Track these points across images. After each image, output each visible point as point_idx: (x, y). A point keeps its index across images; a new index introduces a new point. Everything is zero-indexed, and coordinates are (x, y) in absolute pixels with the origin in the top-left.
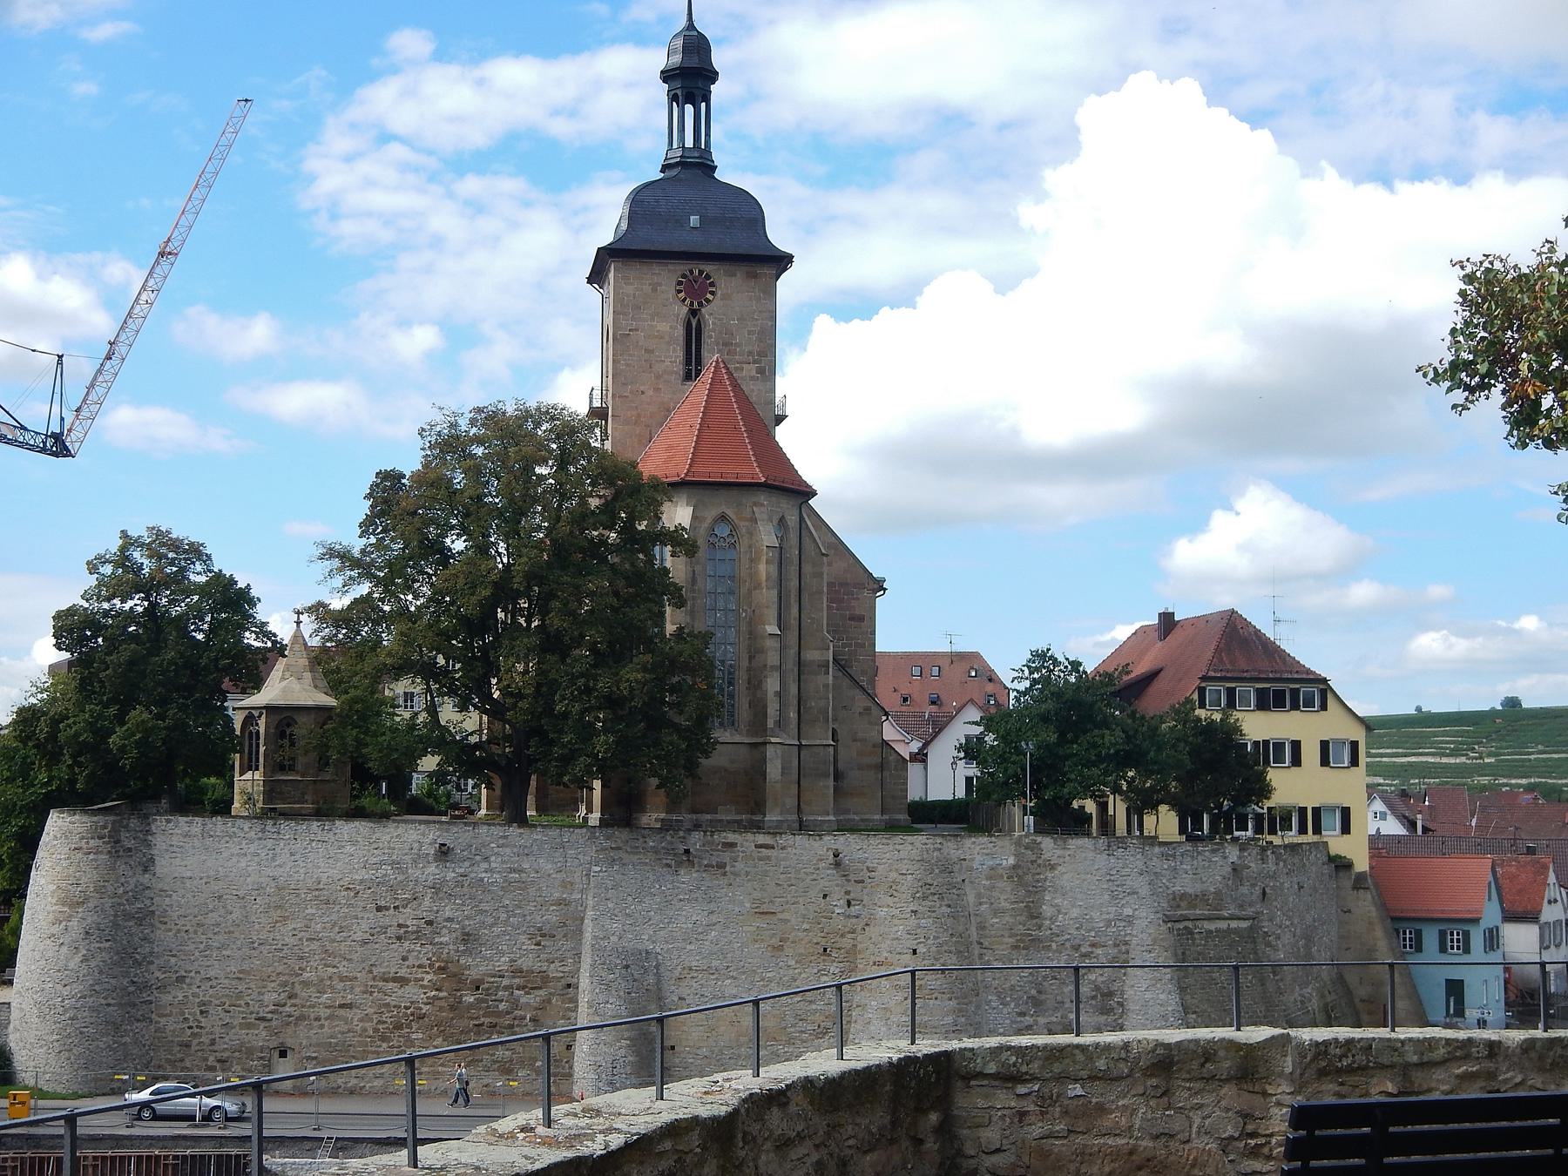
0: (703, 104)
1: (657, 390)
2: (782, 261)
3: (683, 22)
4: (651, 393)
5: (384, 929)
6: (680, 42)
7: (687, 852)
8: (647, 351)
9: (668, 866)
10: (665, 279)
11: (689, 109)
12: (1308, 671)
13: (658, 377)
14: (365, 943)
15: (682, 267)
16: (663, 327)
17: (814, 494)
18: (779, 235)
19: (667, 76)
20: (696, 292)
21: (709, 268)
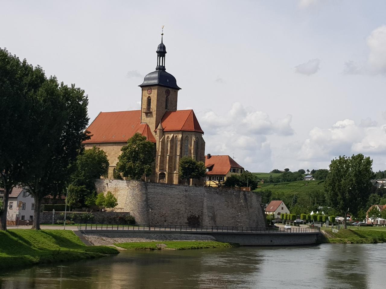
0: (164, 57)
1: (162, 110)
2: (179, 89)
3: (161, 43)
4: (161, 110)
5: (178, 202)
6: (159, 46)
7: (217, 191)
8: (161, 103)
9: (215, 194)
10: (164, 89)
11: (161, 58)
12: (241, 167)
13: (163, 108)
14: (176, 204)
15: (166, 88)
16: (163, 99)
17: (203, 133)
18: (179, 84)
19: (157, 52)
20: (168, 93)
21: (169, 89)
